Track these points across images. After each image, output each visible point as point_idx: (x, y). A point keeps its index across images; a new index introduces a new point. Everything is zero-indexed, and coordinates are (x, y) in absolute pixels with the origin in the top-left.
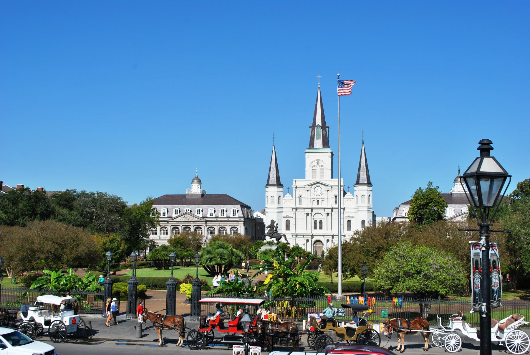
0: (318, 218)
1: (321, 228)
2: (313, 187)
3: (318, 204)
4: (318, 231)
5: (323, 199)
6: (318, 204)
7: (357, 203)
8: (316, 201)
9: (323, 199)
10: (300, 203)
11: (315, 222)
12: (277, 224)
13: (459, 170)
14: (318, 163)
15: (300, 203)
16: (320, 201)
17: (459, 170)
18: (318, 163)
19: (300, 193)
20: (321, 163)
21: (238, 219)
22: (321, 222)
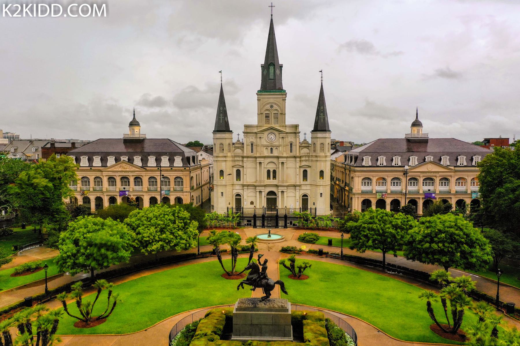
0: (271, 167)
1: (274, 177)
2: (266, 133)
3: (272, 152)
4: (272, 181)
5: (277, 147)
6: (272, 152)
7: (314, 151)
8: (269, 148)
9: (277, 147)
10: (252, 152)
11: (269, 172)
12: (266, 261)
13: (417, 114)
14: (272, 107)
15: (252, 152)
16: (274, 149)
17: (417, 114)
18: (272, 107)
19: (252, 140)
20: (275, 107)
21: (183, 168)
22: (274, 172)
